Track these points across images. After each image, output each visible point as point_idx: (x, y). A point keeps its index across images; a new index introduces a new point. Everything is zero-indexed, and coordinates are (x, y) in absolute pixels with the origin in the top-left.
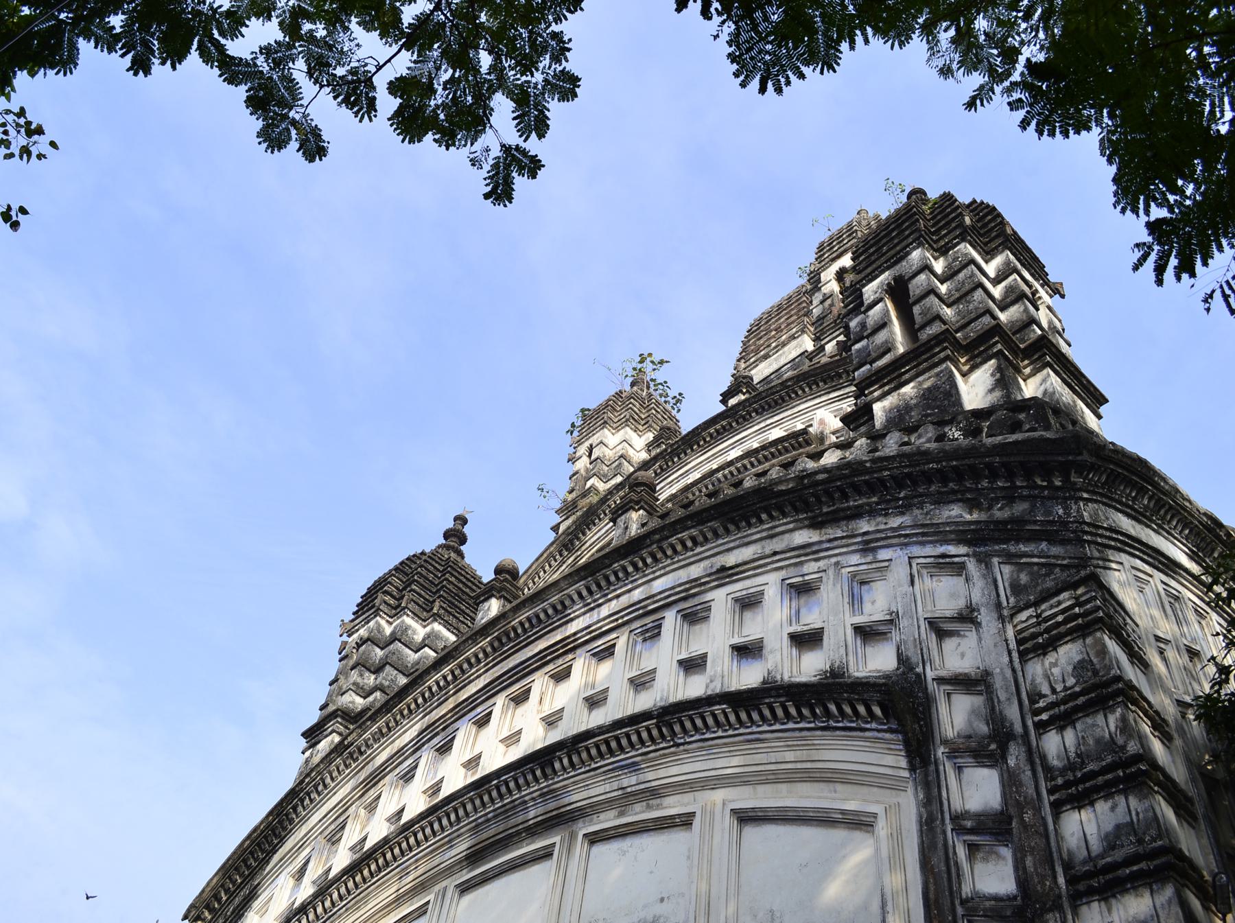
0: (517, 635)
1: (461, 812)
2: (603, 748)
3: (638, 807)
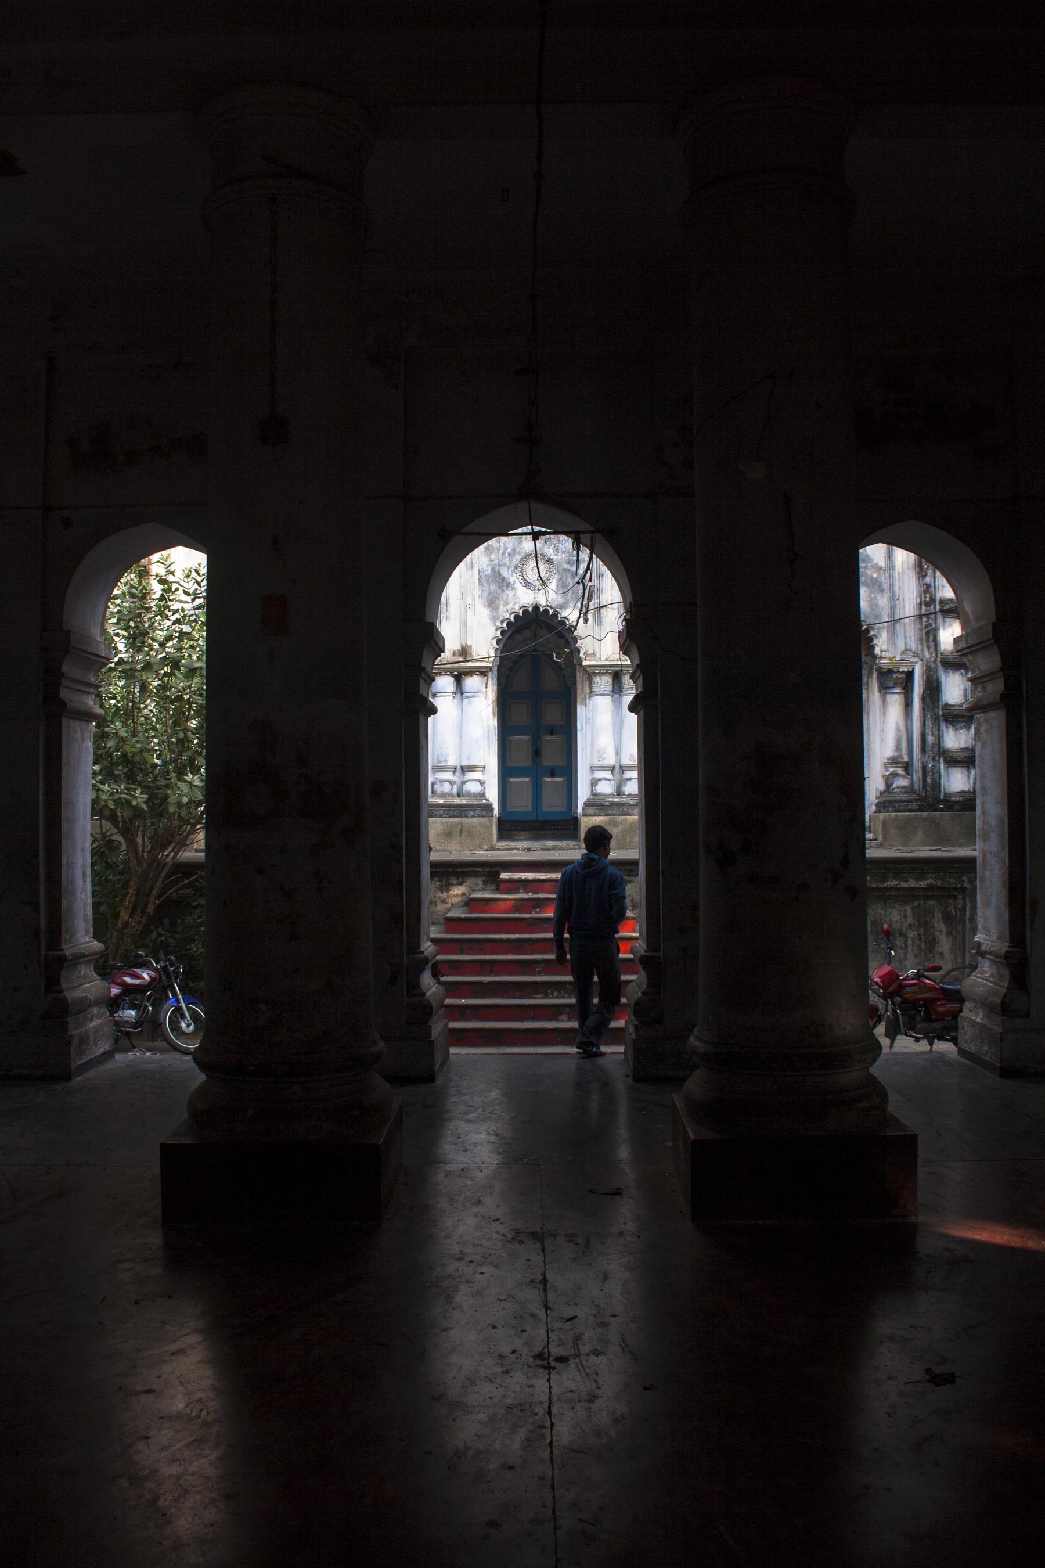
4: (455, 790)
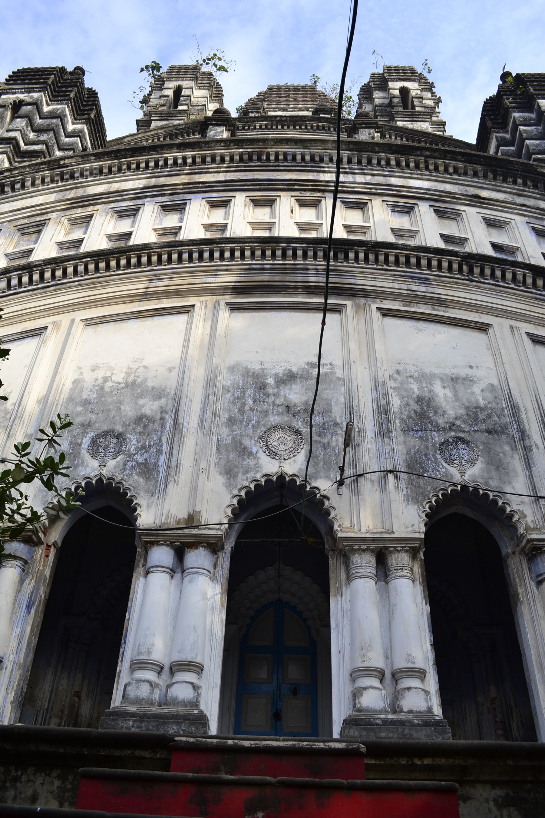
0: (268, 159)
1: (237, 254)
2: (402, 259)
4: (156, 695)
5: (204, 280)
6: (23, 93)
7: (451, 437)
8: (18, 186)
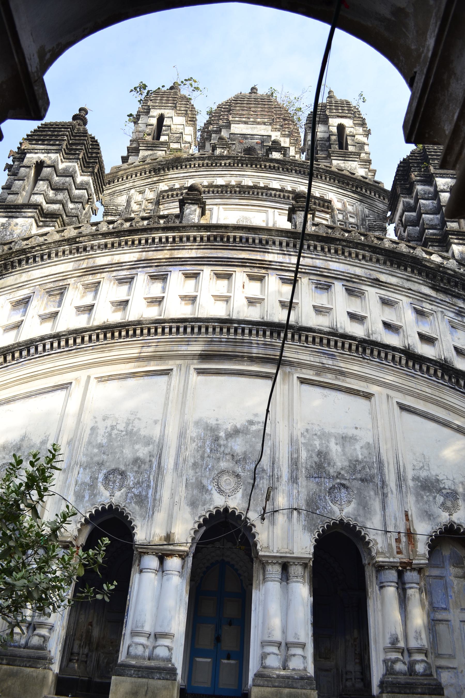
1: (203, 330)
2: (317, 340)
3: (329, 376)
4: (147, 654)
5: (179, 348)
6: (43, 153)
7: (337, 484)
8: (45, 257)
